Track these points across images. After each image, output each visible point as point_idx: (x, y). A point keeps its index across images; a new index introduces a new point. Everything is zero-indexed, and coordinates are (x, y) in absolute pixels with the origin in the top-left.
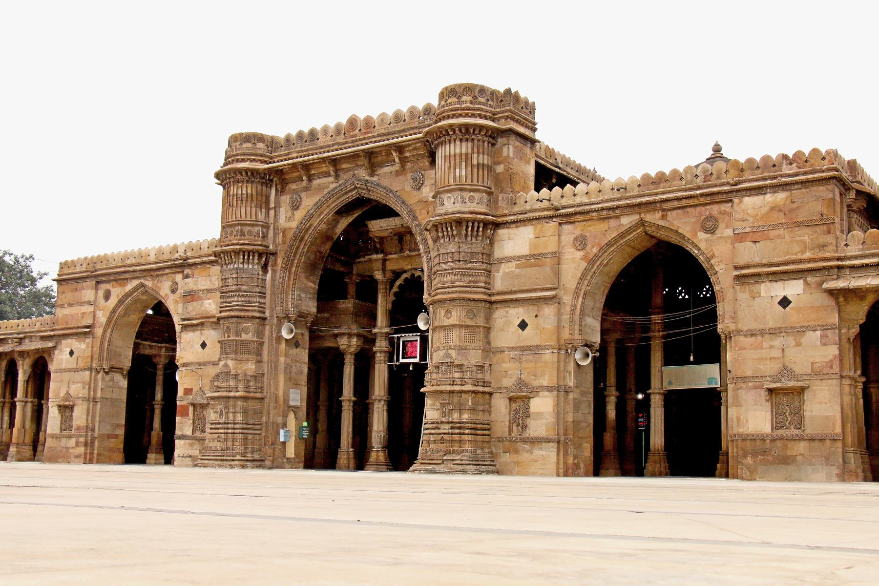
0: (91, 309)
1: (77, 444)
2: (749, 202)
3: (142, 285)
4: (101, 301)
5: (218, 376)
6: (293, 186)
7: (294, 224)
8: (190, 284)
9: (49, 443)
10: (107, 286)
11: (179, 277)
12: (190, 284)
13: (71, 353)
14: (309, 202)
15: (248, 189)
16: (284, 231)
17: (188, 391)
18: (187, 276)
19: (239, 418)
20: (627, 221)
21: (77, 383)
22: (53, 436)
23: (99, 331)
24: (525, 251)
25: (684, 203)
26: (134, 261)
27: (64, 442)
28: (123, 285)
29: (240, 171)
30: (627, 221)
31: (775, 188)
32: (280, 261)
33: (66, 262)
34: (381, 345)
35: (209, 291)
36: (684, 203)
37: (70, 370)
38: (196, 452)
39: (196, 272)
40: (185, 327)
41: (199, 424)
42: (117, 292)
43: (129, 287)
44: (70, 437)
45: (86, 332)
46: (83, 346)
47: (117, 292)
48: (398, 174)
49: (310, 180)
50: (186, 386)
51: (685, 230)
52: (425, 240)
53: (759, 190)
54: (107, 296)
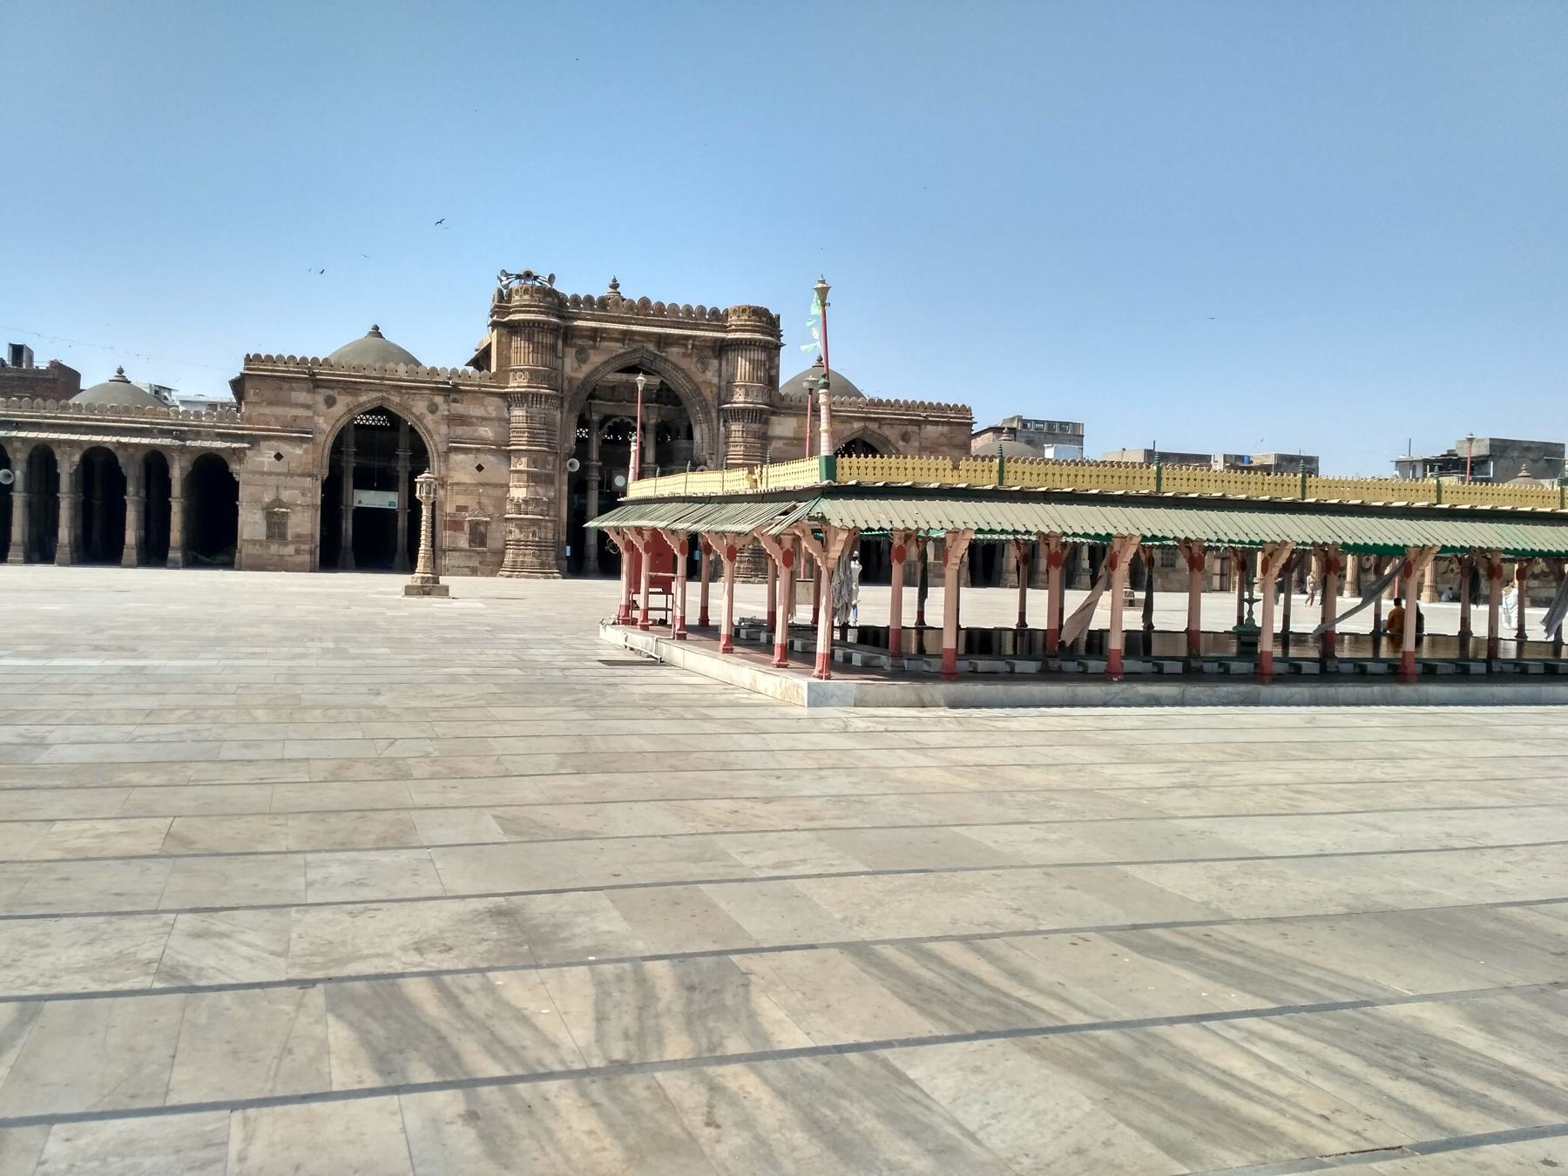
0: (309, 413)
1: (298, 552)
2: (929, 427)
3: (383, 398)
4: (322, 407)
5: (526, 501)
6: (580, 342)
7: (581, 376)
8: (459, 408)
9: (244, 549)
10: (330, 392)
11: (439, 399)
12: (459, 408)
13: (279, 457)
14: (596, 359)
15: (549, 340)
16: (570, 380)
17: (460, 509)
18: (455, 401)
19: (550, 536)
20: (857, 425)
21: (292, 488)
22: (254, 542)
23: (321, 438)
24: (790, 434)
25: (892, 423)
26: (374, 374)
27: (274, 548)
28: (355, 395)
29: (548, 323)
30: (857, 425)
31: (944, 423)
32: (566, 405)
33: (257, 356)
34: (595, 477)
35: (483, 419)
36: (892, 423)
37: (278, 474)
38: (477, 564)
39: (466, 397)
40: (450, 450)
41: (478, 536)
42: (343, 402)
43: (363, 398)
44: (286, 545)
45: (303, 435)
46: (299, 451)
47: (343, 402)
48: (685, 355)
49: (602, 339)
50: (461, 500)
51: (892, 438)
52: (707, 413)
53: (937, 423)
54: (330, 402)
